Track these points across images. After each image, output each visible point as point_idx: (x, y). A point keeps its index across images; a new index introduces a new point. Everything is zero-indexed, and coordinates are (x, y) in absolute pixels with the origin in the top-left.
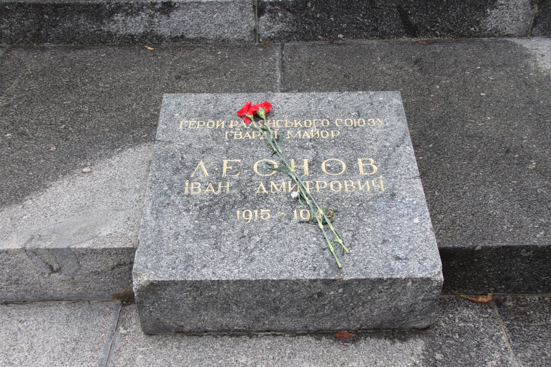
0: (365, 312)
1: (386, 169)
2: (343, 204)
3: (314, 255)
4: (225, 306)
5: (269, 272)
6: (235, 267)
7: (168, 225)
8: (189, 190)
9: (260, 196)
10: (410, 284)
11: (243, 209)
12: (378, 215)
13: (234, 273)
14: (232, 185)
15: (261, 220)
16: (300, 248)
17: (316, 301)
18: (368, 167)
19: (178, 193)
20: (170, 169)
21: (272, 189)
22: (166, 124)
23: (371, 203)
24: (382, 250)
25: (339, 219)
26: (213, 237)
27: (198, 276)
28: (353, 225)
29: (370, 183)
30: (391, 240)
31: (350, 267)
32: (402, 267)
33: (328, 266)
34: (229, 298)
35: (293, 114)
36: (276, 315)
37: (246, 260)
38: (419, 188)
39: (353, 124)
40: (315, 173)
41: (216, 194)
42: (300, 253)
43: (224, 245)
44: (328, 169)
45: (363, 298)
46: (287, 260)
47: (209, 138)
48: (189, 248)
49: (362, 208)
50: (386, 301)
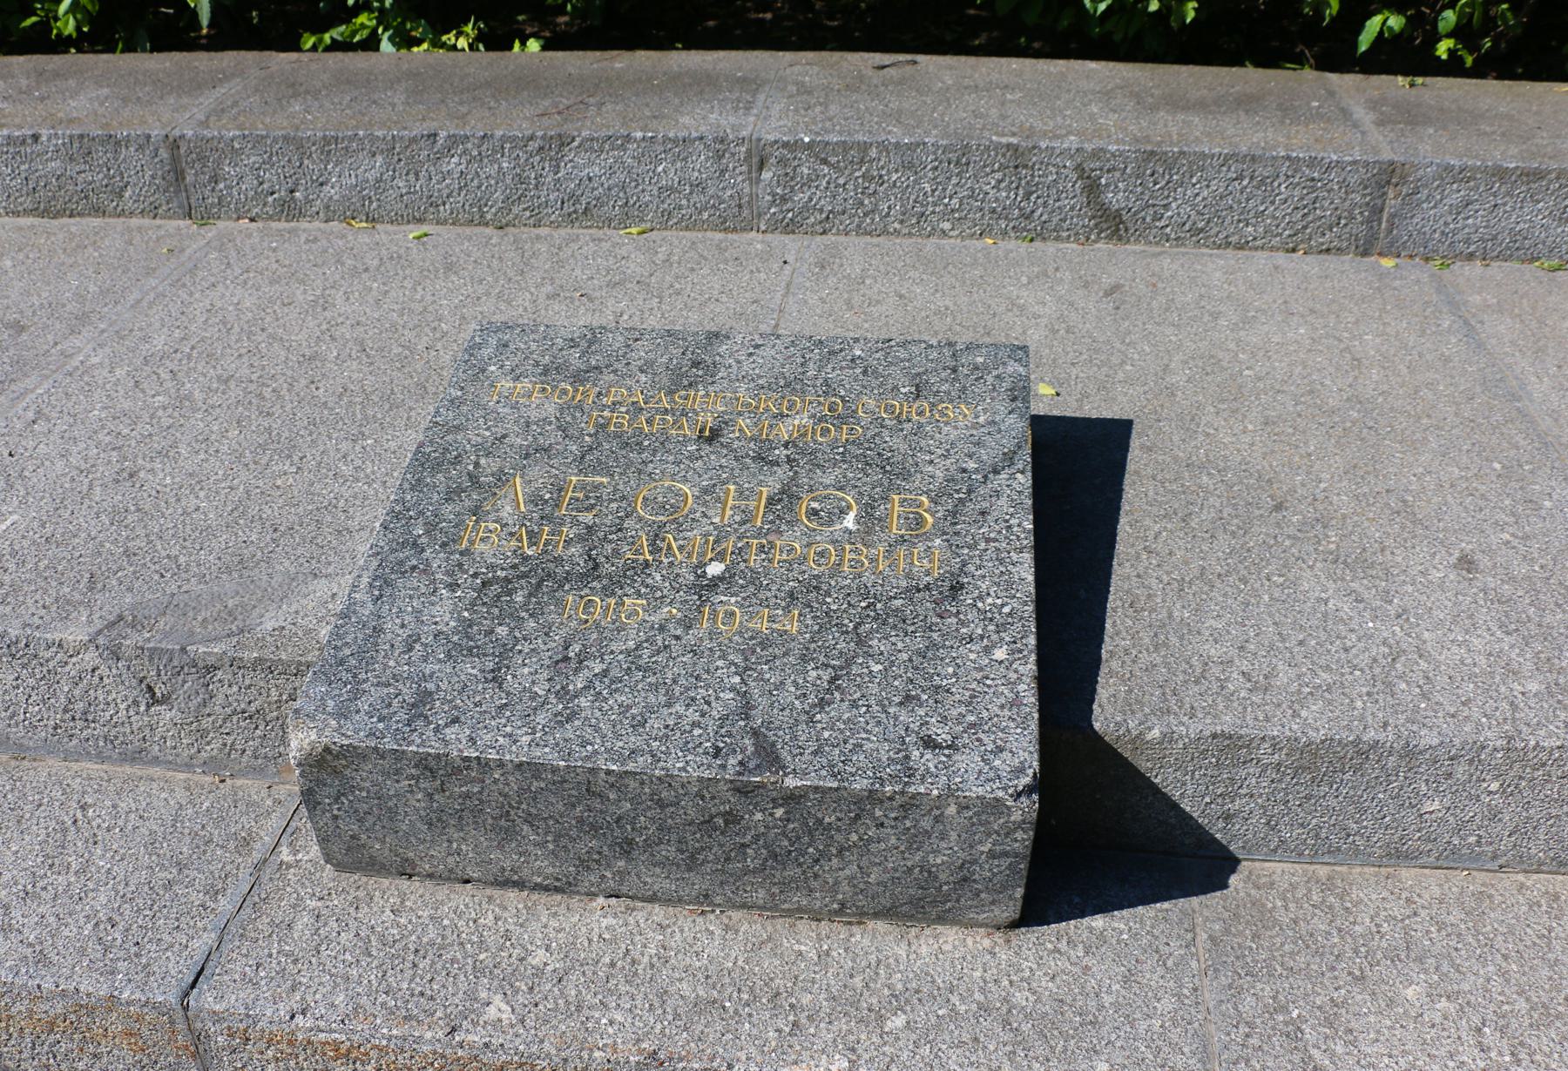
0: (847, 872)
2: (828, 600)
3: (723, 718)
4: (503, 822)
9: (630, 566)
10: (952, 810)
12: (906, 634)
16: (693, 699)
17: (722, 833)
19: (444, 545)
20: (442, 488)
22: (462, 389)
23: (898, 603)
25: (807, 636)
28: (841, 653)
31: (806, 757)
33: (751, 749)
34: (510, 804)
35: (760, 382)
36: (630, 860)
37: (556, 715)
38: (1024, 575)
39: (901, 413)
41: (530, 553)
43: (514, 676)
45: (838, 837)
46: (654, 724)
47: (550, 423)
49: (872, 614)
50: (896, 848)
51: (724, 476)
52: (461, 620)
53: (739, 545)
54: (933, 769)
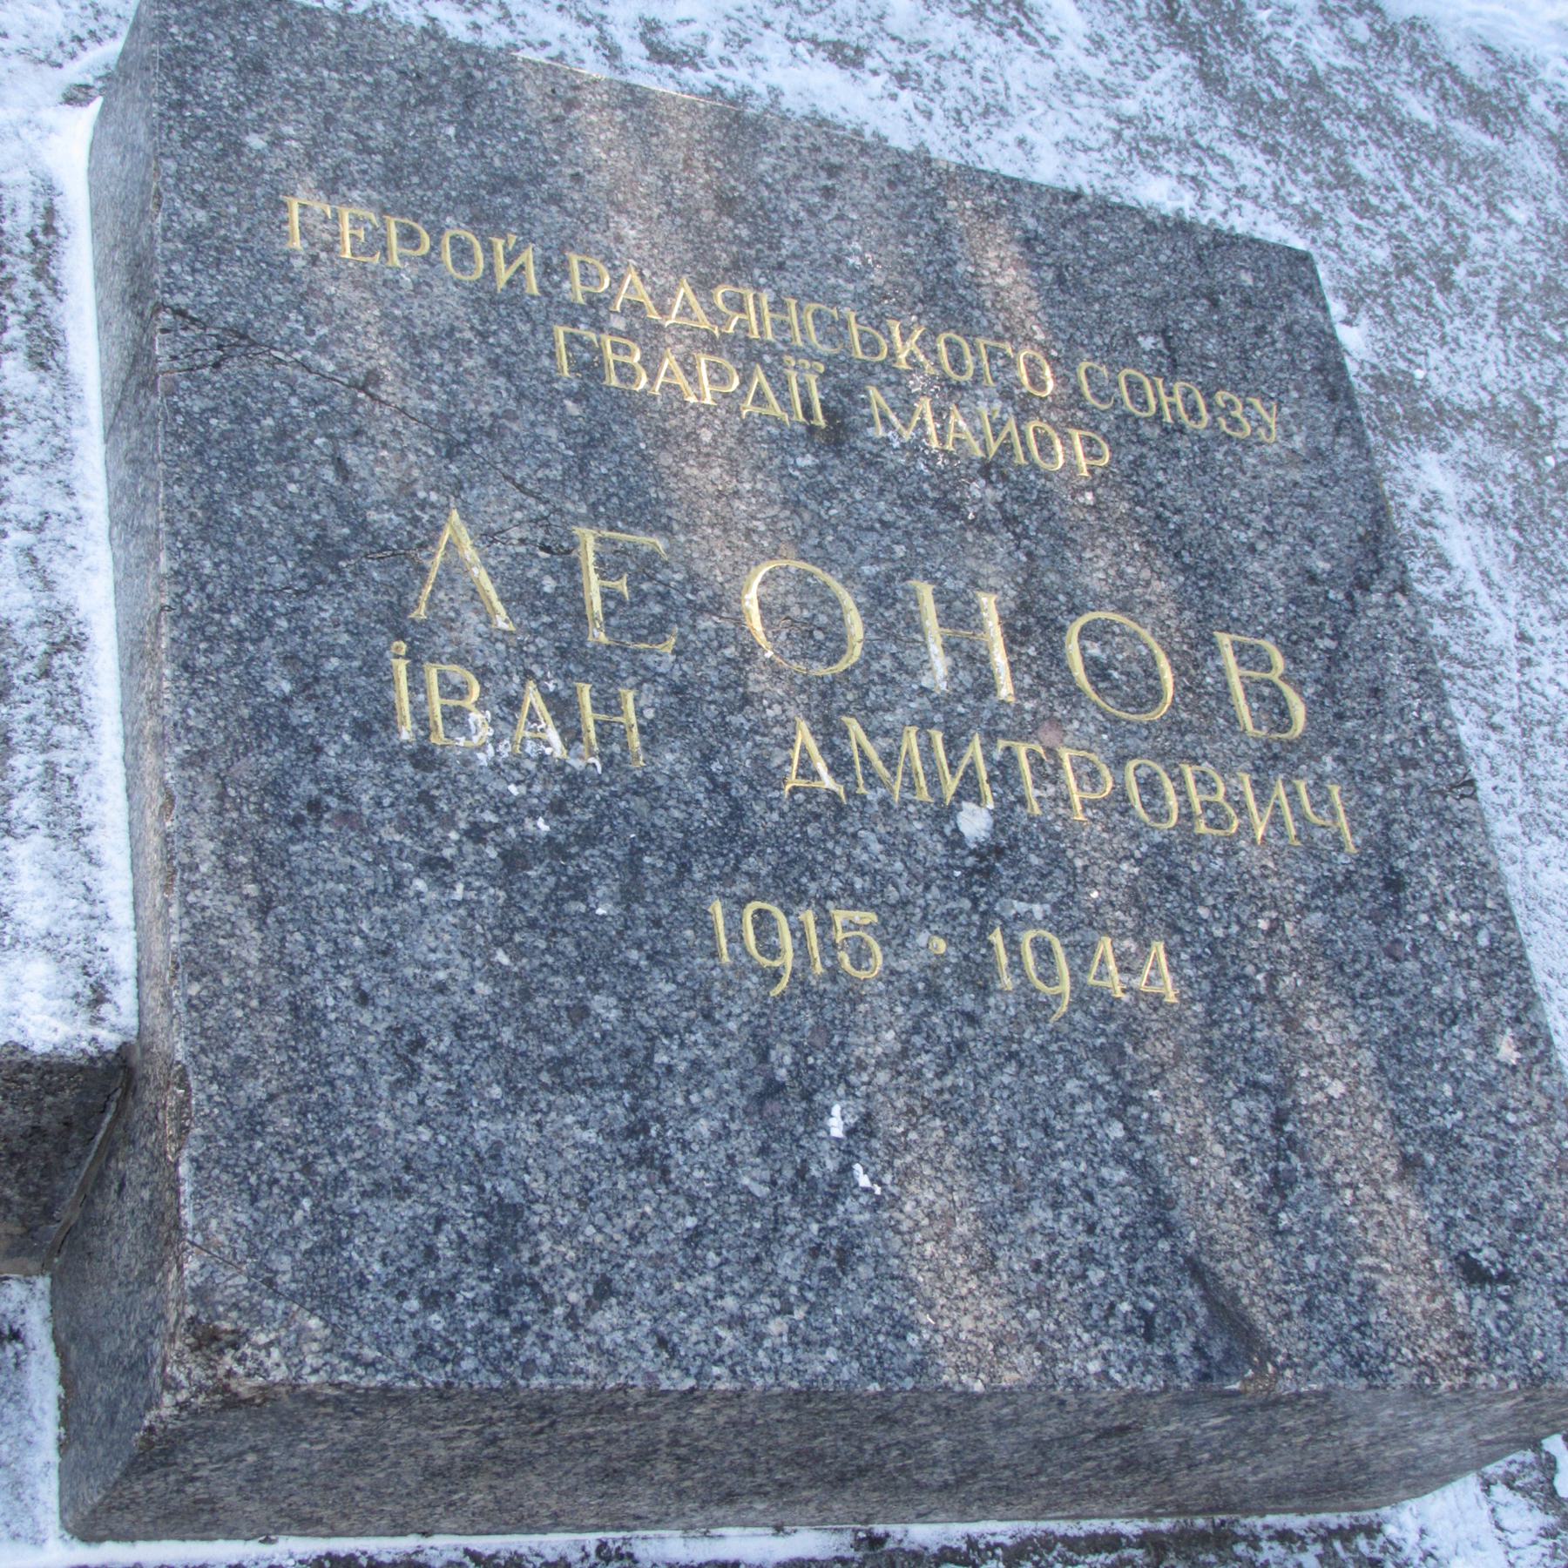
1: (1340, 717)
5: (940, 1340)
6: (765, 1299)
7: (339, 969)
8: (423, 722)
11: (737, 890)
13: (767, 1343)
14: (649, 714)
15: (842, 981)
18: (1266, 691)
19: (362, 730)
21: (858, 767)
22: (203, 201)
24: (1405, 1220)
26: (612, 1077)
27: (581, 1362)
29: (1293, 795)
30: (1430, 1159)
32: (1498, 1327)
33: (1201, 1310)
39: (1159, 409)
40: (1044, 695)
42: (1065, 1219)
43: (685, 1146)
44: (1098, 671)
48: (496, 1152)
49: (1284, 948)
51: (900, 551)
52: (498, 976)
53: (997, 755)
54: (1496, 1334)
